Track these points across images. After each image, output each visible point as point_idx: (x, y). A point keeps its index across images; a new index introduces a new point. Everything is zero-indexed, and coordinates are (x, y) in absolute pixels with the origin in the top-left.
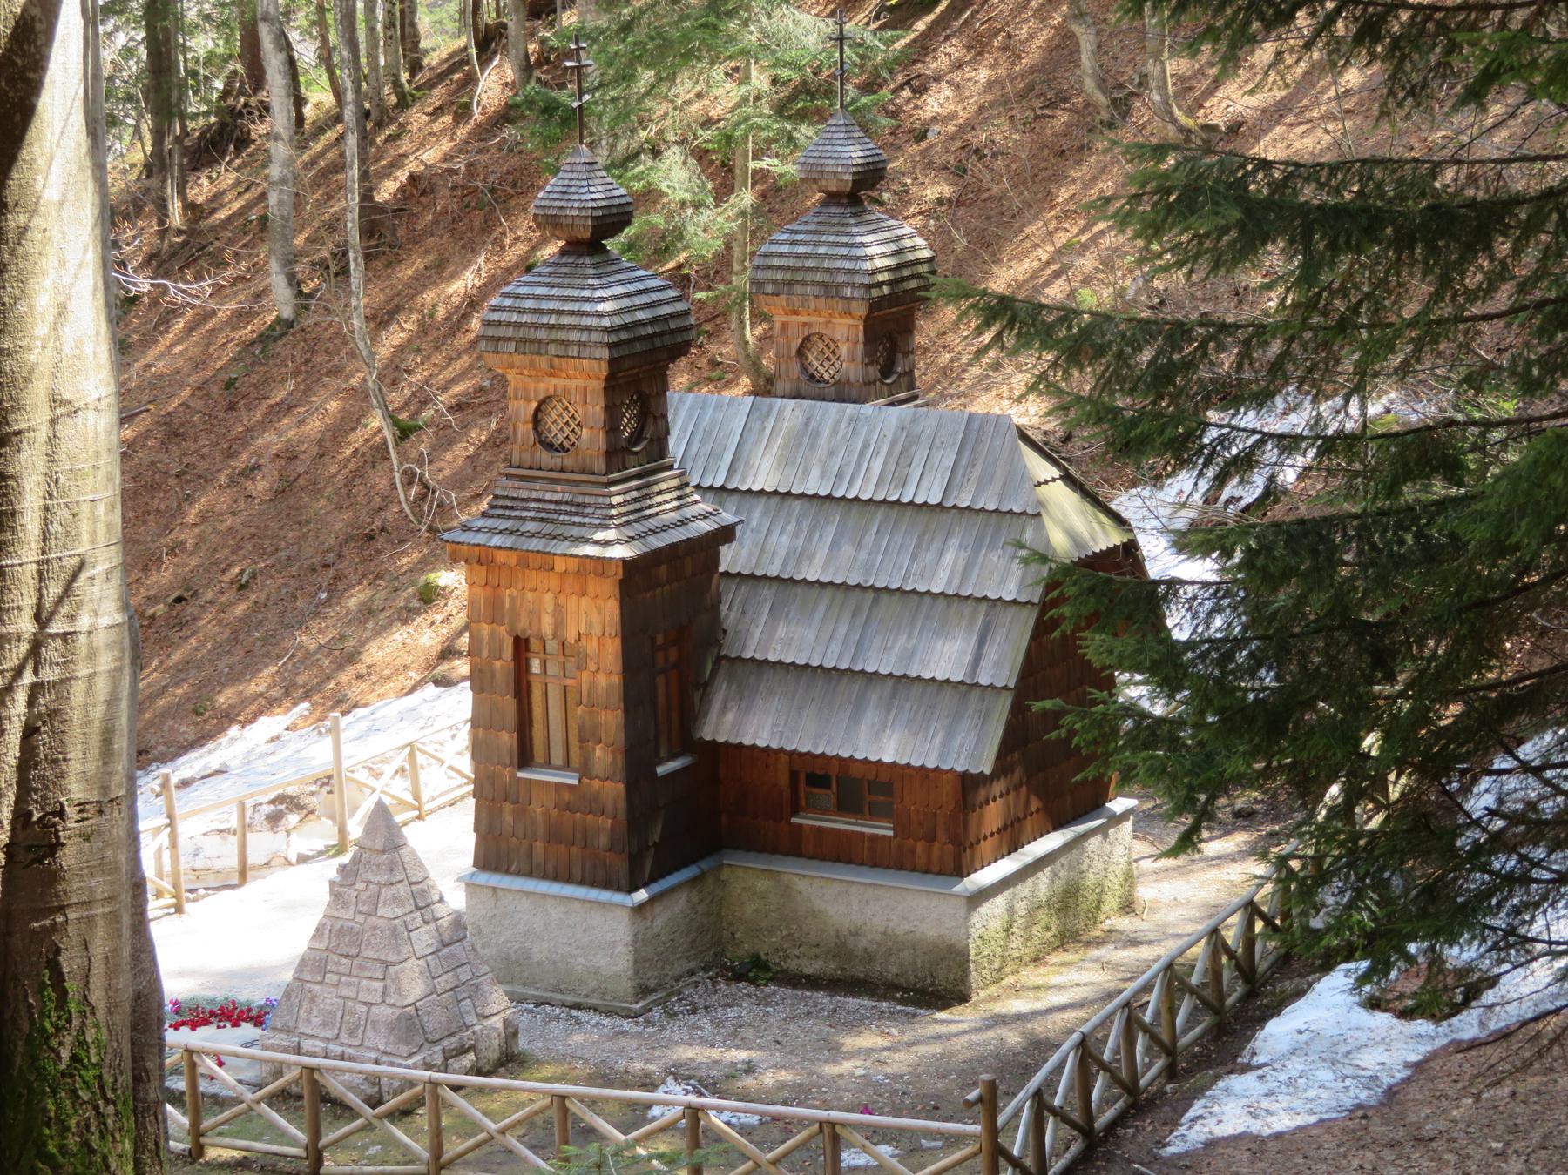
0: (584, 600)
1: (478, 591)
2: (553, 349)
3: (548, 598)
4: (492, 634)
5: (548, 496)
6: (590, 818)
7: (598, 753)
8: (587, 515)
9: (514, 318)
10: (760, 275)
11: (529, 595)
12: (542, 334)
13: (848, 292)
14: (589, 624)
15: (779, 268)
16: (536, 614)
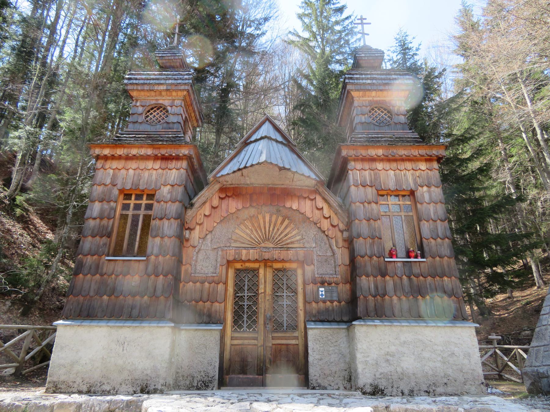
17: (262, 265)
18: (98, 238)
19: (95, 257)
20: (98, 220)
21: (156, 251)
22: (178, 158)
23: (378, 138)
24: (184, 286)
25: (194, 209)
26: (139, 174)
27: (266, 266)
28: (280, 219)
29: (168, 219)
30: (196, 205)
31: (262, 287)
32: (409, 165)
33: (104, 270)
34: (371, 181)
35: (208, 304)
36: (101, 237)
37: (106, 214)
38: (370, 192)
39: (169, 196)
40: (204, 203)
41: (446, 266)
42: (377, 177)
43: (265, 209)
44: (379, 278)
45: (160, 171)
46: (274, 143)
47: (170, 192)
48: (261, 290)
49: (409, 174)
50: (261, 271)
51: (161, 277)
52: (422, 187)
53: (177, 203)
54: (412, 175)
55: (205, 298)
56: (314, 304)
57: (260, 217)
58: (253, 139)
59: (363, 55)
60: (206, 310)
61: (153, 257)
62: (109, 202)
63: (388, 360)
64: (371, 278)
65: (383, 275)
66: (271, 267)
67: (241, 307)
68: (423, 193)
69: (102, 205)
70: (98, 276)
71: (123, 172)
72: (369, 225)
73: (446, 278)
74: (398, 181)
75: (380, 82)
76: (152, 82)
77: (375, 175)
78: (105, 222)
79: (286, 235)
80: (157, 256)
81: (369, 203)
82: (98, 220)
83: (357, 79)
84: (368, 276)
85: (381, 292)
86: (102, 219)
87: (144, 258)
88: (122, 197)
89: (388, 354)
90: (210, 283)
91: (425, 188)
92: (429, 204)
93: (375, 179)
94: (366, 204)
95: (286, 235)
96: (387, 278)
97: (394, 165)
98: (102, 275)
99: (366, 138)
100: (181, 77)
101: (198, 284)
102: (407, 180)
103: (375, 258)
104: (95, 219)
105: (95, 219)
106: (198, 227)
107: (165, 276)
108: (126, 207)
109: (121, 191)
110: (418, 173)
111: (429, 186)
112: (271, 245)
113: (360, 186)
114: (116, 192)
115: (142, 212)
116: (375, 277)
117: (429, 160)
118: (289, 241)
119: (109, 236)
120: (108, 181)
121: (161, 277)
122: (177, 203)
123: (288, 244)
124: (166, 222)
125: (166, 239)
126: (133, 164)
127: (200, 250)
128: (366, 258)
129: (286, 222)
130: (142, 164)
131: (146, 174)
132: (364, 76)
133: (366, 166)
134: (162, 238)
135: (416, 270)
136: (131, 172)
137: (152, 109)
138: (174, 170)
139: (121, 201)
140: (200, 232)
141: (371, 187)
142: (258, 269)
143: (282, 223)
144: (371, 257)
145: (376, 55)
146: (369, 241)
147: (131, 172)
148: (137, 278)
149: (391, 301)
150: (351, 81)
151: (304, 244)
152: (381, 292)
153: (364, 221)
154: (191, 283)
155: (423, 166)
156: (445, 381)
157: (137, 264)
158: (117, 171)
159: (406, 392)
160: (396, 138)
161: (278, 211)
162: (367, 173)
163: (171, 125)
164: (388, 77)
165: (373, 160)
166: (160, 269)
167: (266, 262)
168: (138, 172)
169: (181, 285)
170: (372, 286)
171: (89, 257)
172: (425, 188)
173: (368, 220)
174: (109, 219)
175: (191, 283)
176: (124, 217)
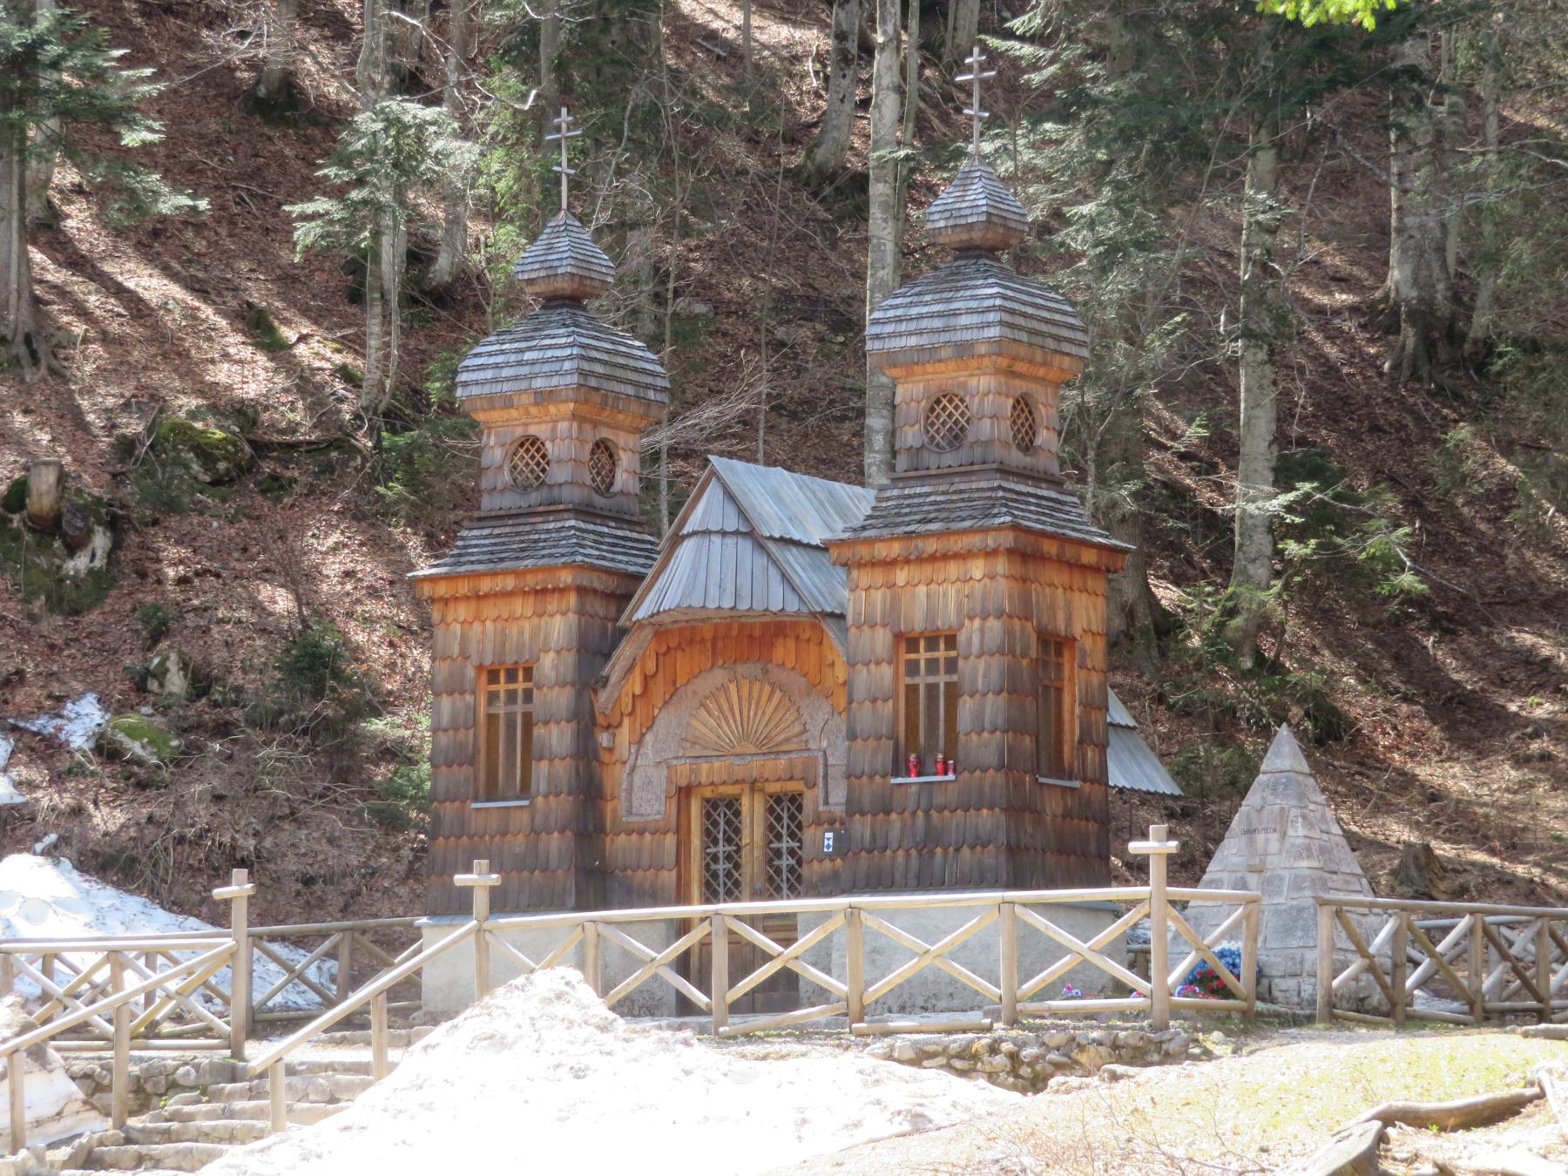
0: (1084, 595)
1: (1013, 583)
2: (1051, 344)
3: (1060, 591)
4: (1023, 629)
5: (1040, 492)
6: (1083, 823)
7: (1090, 754)
8: (1068, 513)
9: (1023, 308)
10: (586, 366)
11: (1048, 589)
12: (1044, 328)
13: (651, 394)
14: (1089, 622)
15: (599, 361)
16: (1052, 609)
17: (746, 787)
18: (455, 767)
19: (457, 804)
20: (451, 732)
21: (543, 787)
22: (560, 591)
23: (920, 495)
24: (613, 841)
25: (609, 688)
26: (503, 630)
27: (753, 790)
28: (767, 688)
29: (558, 723)
30: (613, 679)
31: (746, 832)
32: (953, 569)
33: (473, 830)
34: (883, 615)
35: (651, 873)
36: (461, 765)
37: (461, 720)
38: (881, 639)
39: (553, 675)
40: (631, 668)
41: (987, 789)
42: (894, 605)
43: (741, 669)
44: (881, 816)
45: (535, 620)
46: (717, 540)
47: (556, 667)
48: (745, 840)
49: (951, 591)
50: (745, 801)
51: (556, 834)
52: (971, 619)
53: (568, 688)
54: (958, 592)
55: (645, 861)
56: (816, 865)
57: (732, 688)
58: (685, 531)
59: (942, 224)
60: (647, 886)
61: (540, 799)
62: (462, 693)
63: (873, 961)
64: (869, 817)
65: (888, 812)
66: (761, 790)
67: (715, 875)
68: (971, 634)
69: (454, 702)
70: (465, 838)
71: (477, 627)
72: (874, 711)
73: (985, 811)
74: (931, 612)
75: (935, 339)
76: (506, 387)
77: (893, 599)
78: (462, 734)
79: (777, 726)
80: (546, 796)
81: (878, 663)
82: (451, 732)
83: (892, 335)
84: (863, 814)
85: (879, 843)
86: (456, 729)
87: (526, 803)
88: (484, 677)
89: (875, 951)
90: (653, 834)
91: (977, 622)
92: (979, 657)
93: (892, 607)
94: (872, 666)
95: (777, 726)
96: (894, 816)
97: (927, 570)
98: (471, 837)
99: (899, 497)
100: (556, 366)
101: (634, 836)
102: (946, 605)
103: (877, 778)
104: (446, 730)
105: (446, 730)
106: (626, 721)
107: (562, 831)
108: (492, 697)
109: (480, 668)
110: (967, 588)
111: (984, 618)
112: (753, 750)
113: (865, 628)
114: (470, 672)
115: (519, 708)
116: (875, 815)
117: (990, 554)
118: (782, 737)
119: (472, 761)
120: (456, 650)
121: (556, 834)
122: (568, 688)
123: (781, 743)
124: (554, 728)
125: (557, 762)
126: (489, 609)
127: (633, 768)
128: (865, 778)
129: (778, 694)
130: (502, 608)
131: (513, 630)
132: (903, 327)
133: (878, 576)
134: (551, 760)
135: (939, 799)
136: (489, 624)
137: (522, 445)
138: (558, 617)
139: (484, 688)
140: (632, 731)
141: (884, 626)
142: (737, 799)
143: (769, 700)
144: (871, 777)
145: (970, 220)
146: (872, 743)
147: (489, 624)
148: (520, 838)
149: (894, 859)
150: (877, 345)
151: (807, 742)
152: (879, 843)
153: (867, 703)
154: (623, 836)
155: (977, 569)
156: (951, 990)
157: (519, 812)
158: (467, 626)
159: (895, 1008)
160: (955, 492)
161: (766, 672)
162: (878, 596)
163: (556, 492)
164: (952, 321)
165: (889, 564)
166: (553, 819)
167: (754, 786)
168: (500, 625)
169: (608, 840)
170: (868, 833)
171: (448, 804)
172: (977, 622)
173: (874, 701)
174: (467, 729)
175: (623, 836)
176: (492, 719)
